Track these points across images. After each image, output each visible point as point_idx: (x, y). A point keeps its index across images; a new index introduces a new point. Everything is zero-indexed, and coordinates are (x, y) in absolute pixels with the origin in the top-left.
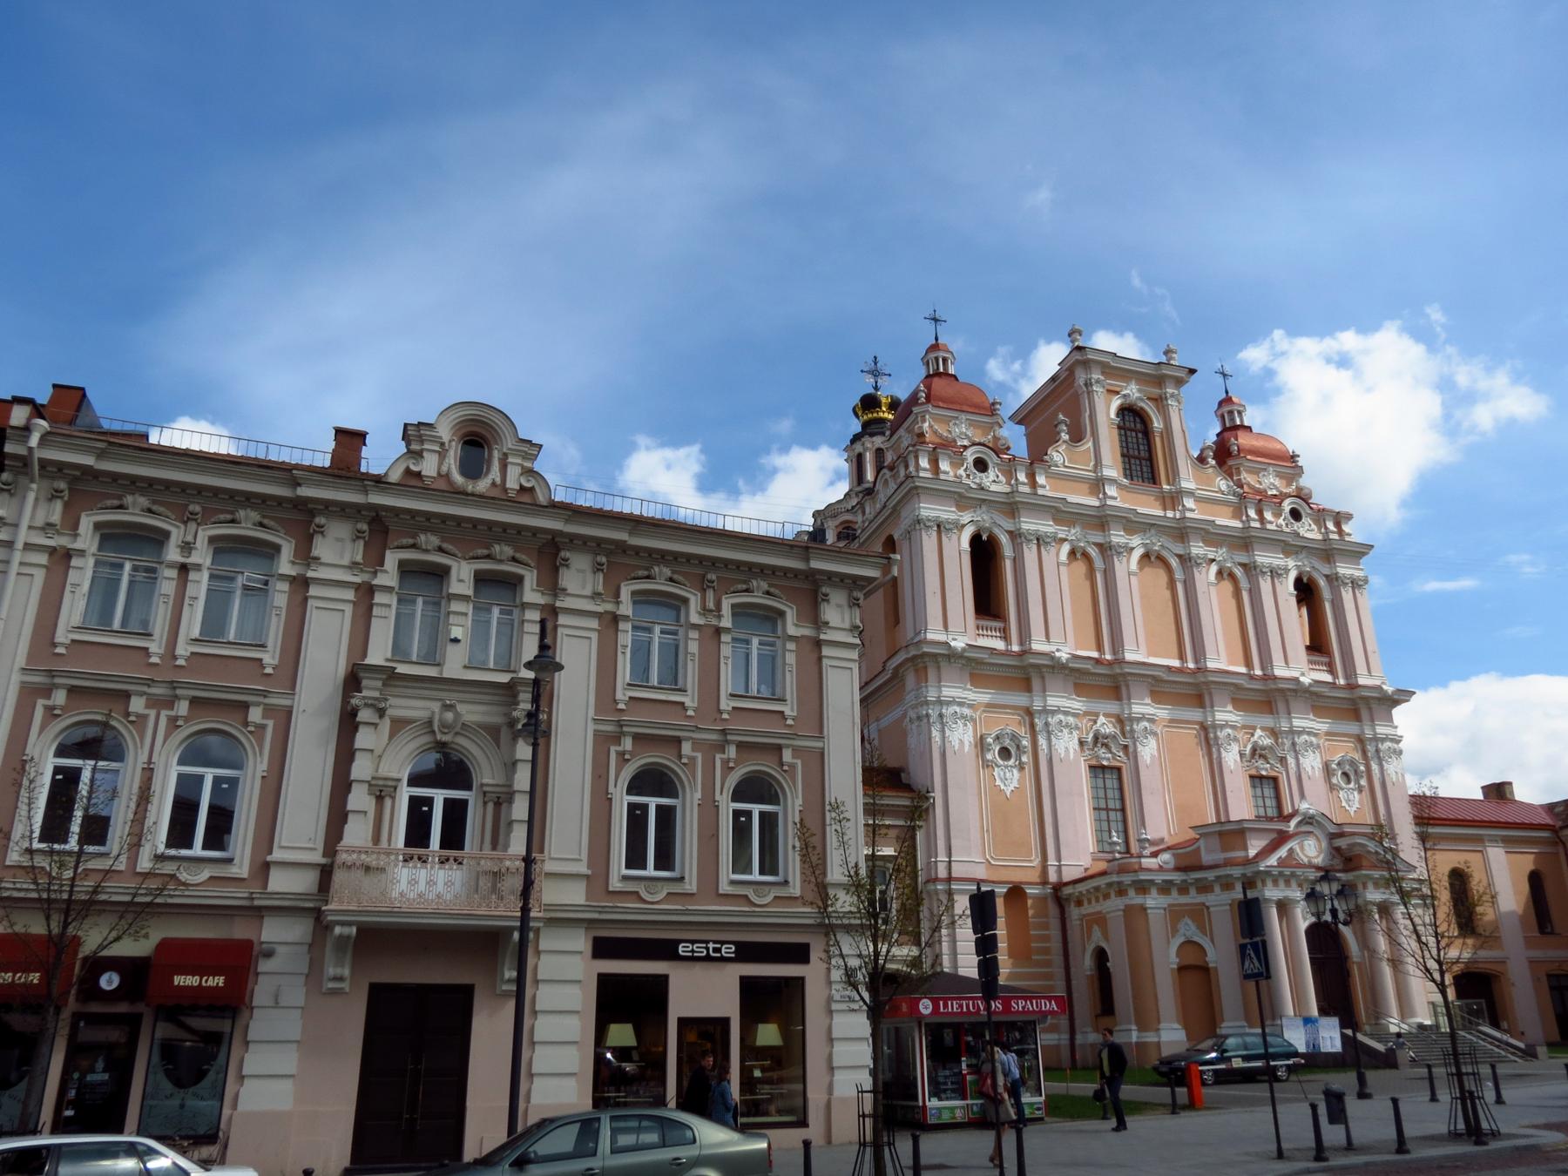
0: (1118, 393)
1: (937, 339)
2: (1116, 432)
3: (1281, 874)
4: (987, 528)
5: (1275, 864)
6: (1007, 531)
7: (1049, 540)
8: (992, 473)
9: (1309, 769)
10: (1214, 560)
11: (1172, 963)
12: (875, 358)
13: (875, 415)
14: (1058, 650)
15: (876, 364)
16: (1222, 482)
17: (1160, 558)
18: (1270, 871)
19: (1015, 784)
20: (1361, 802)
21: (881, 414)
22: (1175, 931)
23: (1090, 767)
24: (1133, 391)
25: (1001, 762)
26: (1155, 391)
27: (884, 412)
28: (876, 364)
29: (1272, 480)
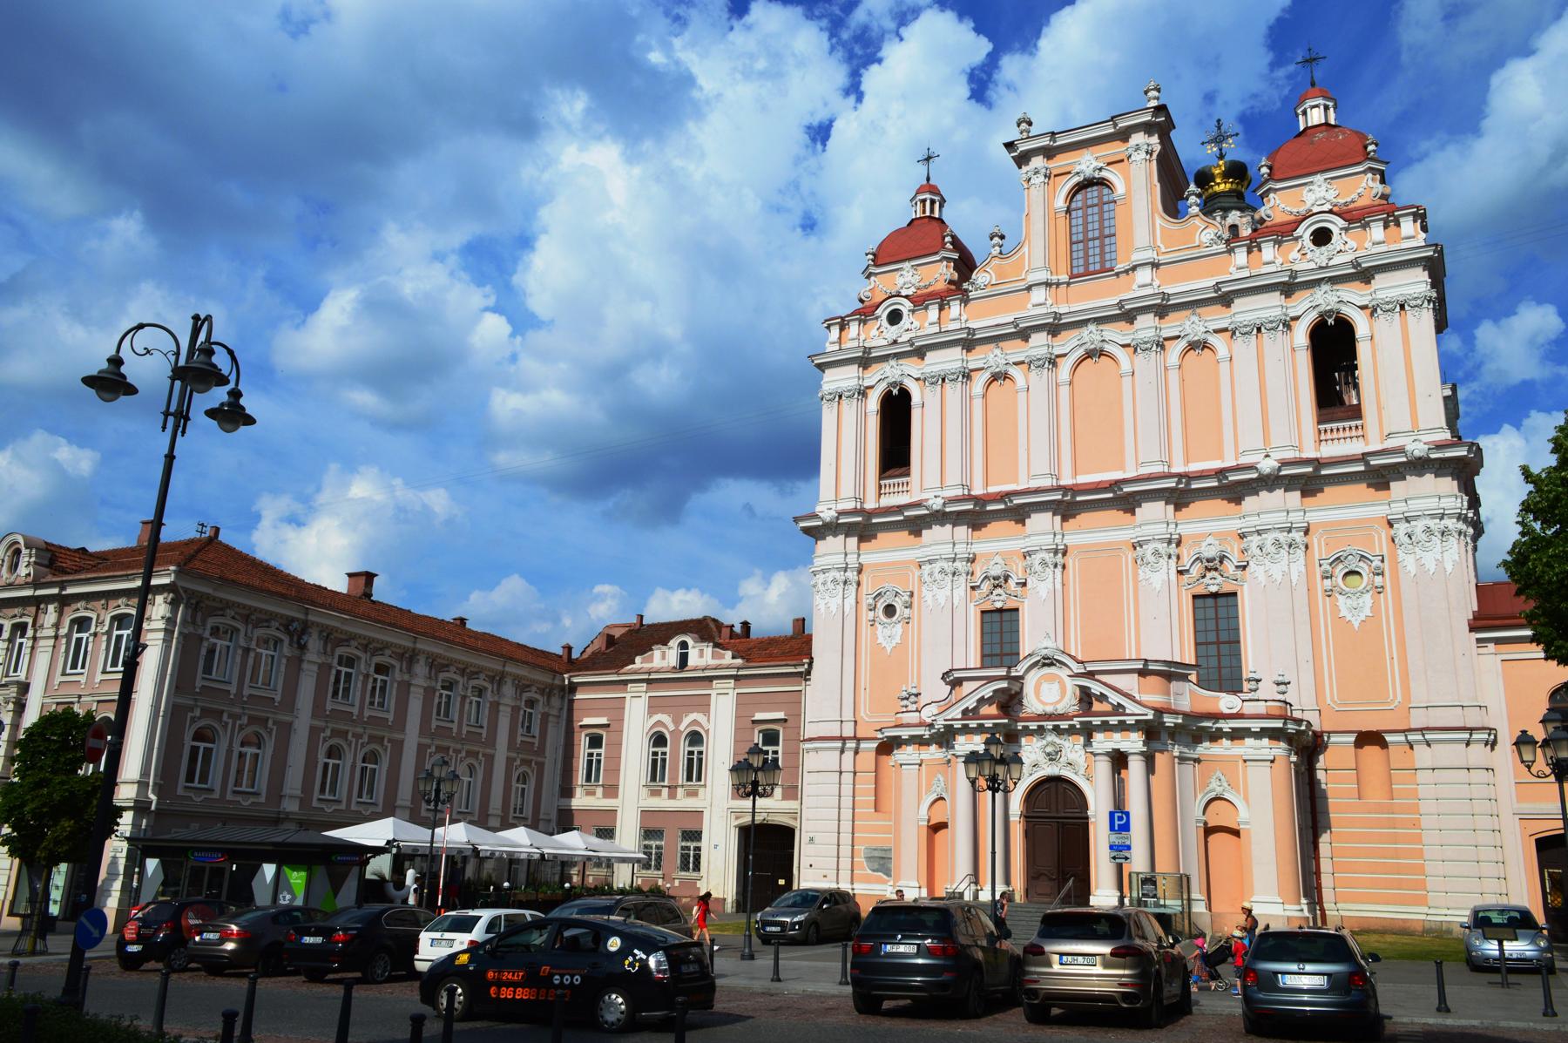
0: (1069, 173)
1: (928, 179)
2: (1062, 222)
3: (965, 726)
4: (895, 382)
5: (959, 716)
6: (918, 379)
7: (952, 377)
8: (906, 322)
9: (1278, 576)
10: (1178, 337)
11: (923, 820)
12: (1219, 121)
13: (1210, 191)
14: (936, 497)
15: (1219, 128)
16: (1205, 232)
17: (1101, 353)
18: (952, 725)
19: (898, 640)
20: (1375, 607)
21: (1217, 188)
22: (929, 785)
23: (983, 612)
24: (1086, 163)
25: (885, 620)
26: (1115, 149)
27: (1218, 184)
28: (1219, 128)
29: (1323, 194)
